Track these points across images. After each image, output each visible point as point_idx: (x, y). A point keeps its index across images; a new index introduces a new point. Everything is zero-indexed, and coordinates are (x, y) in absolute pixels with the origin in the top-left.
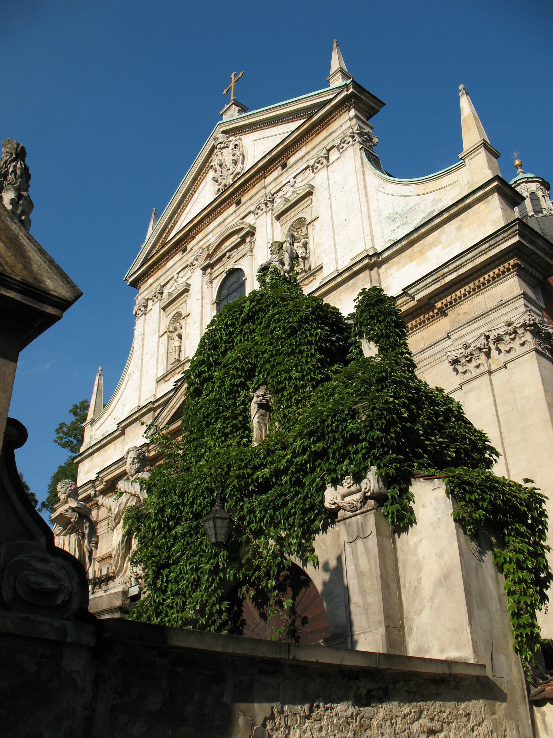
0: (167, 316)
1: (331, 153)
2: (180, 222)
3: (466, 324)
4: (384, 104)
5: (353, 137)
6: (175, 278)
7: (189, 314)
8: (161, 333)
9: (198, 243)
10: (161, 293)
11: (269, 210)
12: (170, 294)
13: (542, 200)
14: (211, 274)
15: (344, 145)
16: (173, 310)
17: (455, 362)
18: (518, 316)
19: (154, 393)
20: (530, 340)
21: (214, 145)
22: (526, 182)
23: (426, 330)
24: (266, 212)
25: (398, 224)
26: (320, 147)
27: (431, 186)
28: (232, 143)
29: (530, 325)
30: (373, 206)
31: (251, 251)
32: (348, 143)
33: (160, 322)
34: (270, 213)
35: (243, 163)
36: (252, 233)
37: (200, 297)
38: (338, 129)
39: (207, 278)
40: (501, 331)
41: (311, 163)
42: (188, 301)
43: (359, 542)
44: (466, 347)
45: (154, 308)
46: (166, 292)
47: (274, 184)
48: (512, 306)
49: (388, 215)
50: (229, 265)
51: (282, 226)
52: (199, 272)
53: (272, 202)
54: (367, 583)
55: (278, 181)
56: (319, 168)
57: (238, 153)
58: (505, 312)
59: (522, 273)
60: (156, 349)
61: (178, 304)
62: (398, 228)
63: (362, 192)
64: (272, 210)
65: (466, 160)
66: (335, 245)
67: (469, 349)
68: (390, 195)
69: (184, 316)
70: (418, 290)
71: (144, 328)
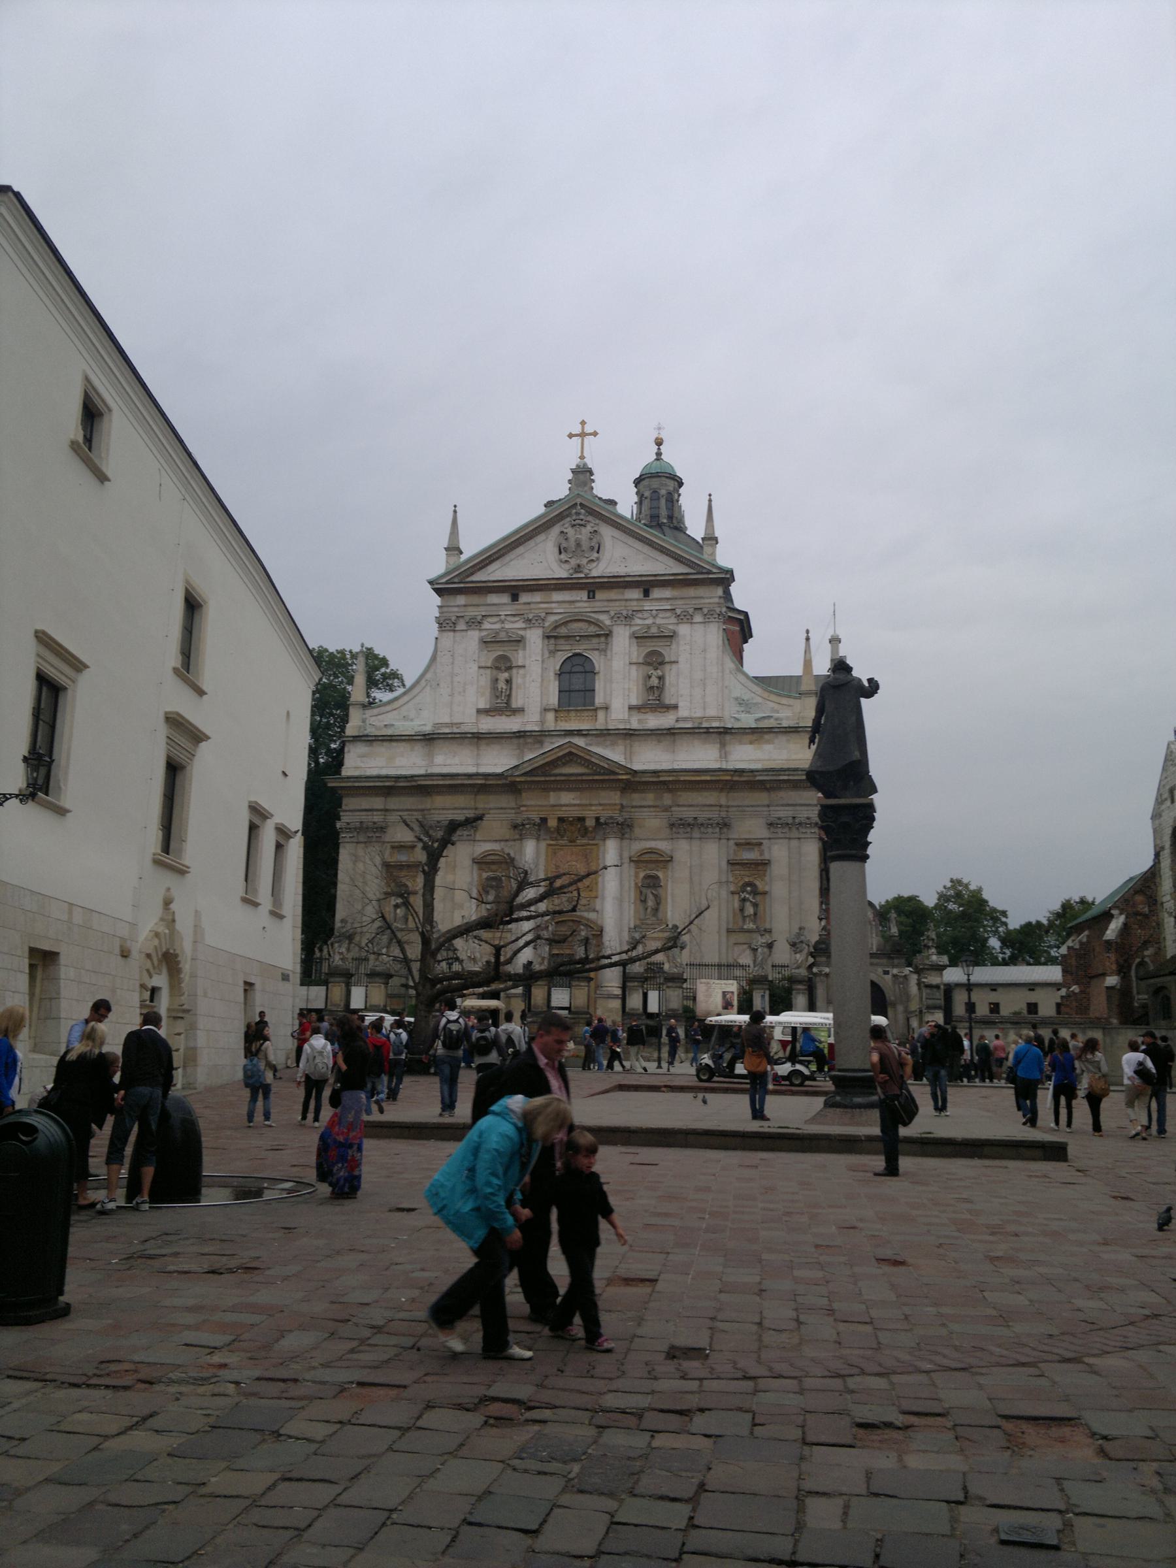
2: (507, 558)
8: (483, 665)
12: (497, 633)
25: (742, 709)
26: (688, 601)
27: (773, 697)
31: (605, 650)
36: (608, 635)
39: (552, 648)
41: (678, 611)
44: (779, 819)
45: (469, 632)
46: (486, 625)
47: (635, 603)
48: (810, 808)
55: (642, 603)
57: (595, 540)
61: (506, 649)
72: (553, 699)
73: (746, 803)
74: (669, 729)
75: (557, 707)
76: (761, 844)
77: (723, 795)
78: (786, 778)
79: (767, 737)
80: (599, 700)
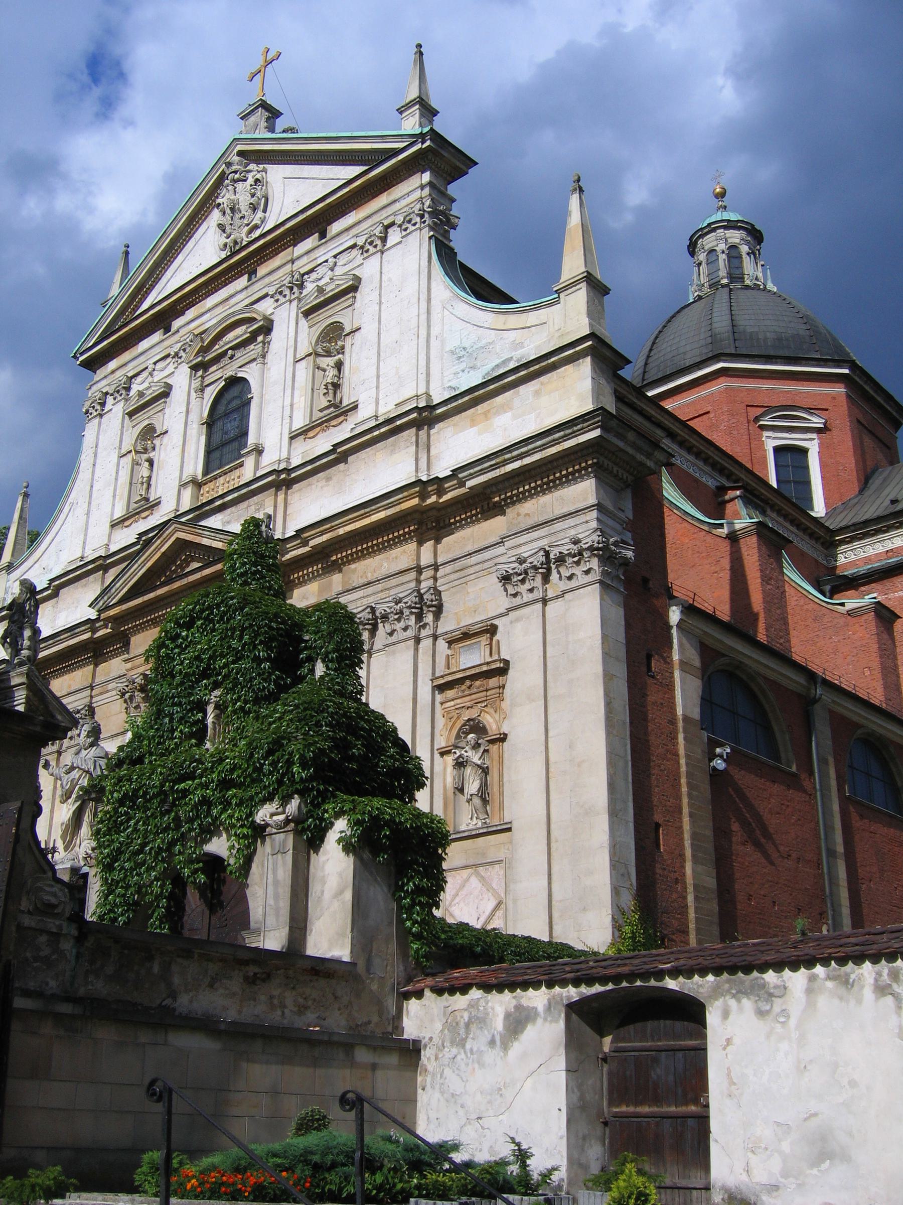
0: (133, 427)
1: (390, 231)
3: (526, 530)
4: (476, 163)
5: (422, 216)
6: (150, 369)
7: (166, 432)
8: (123, 451)
9: (188, 323)
10: (128, 389)
11: (294, 299)
12: (141, 394)
13: (746, 260)
14: (203, 377)
15: (408, 225)
16: (143, 420)
17: (506, 579)
18: (588, 533)
19: (106, 542)
20: (596, 568)
21: (223, 173)
22: (725, 227)
23: (477, 526)
24: (291, 301)
25: (463, 365)
26: (376, 218)
28: (252, 174)
29: (598, 549)
30: (435, 331)
31: (264, 356)
32: (414, 224)
33: (122, 434)
34: (295, 303)
35: (265, 211)
36: (267, 328)
37: (184, 409)
38: (403, 197)
39: (196, 384)
40: (564, 550)
41: (360, 241)
42: (167, 410)
43: (279, 856)
44: (521, 561)
45: (115, 409)
46: (135, 388)
47: (305, 260)
49: (453, 349)
50: (230, 370)
51: (310, 327)
52: (185, 369)
53: (301, 286)
54: (280, 890)
55: (313, 255)
56: (370, 252)
57: (259, 194)
58: (573, 525)
59: (602, 474)
60: (114, 474)
61: (152, 412)
62: (463, 371)
63: (424, 305)
64: (300, 300)
65: (562, 295)
66: (378, 377)
67: (524, 565)
68: (459, 318)
69: (158, 432)
70: (471, 474)
71: (98, 438)
72: (195, 466)
73: (470, 548)
74: (336, 446)
75: (200, 477)
76: (492, 630)
77: (429, 544)
78: (517, 465)
79: (499, 399)
80: (251, 440)
